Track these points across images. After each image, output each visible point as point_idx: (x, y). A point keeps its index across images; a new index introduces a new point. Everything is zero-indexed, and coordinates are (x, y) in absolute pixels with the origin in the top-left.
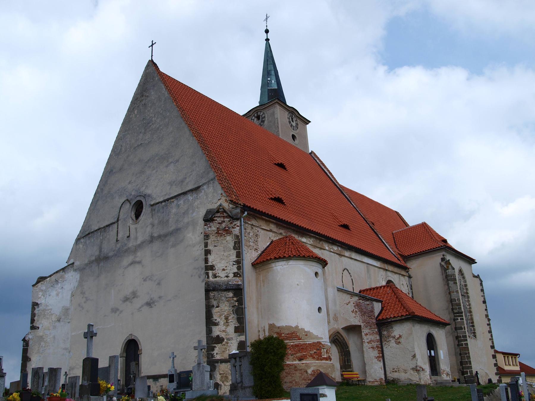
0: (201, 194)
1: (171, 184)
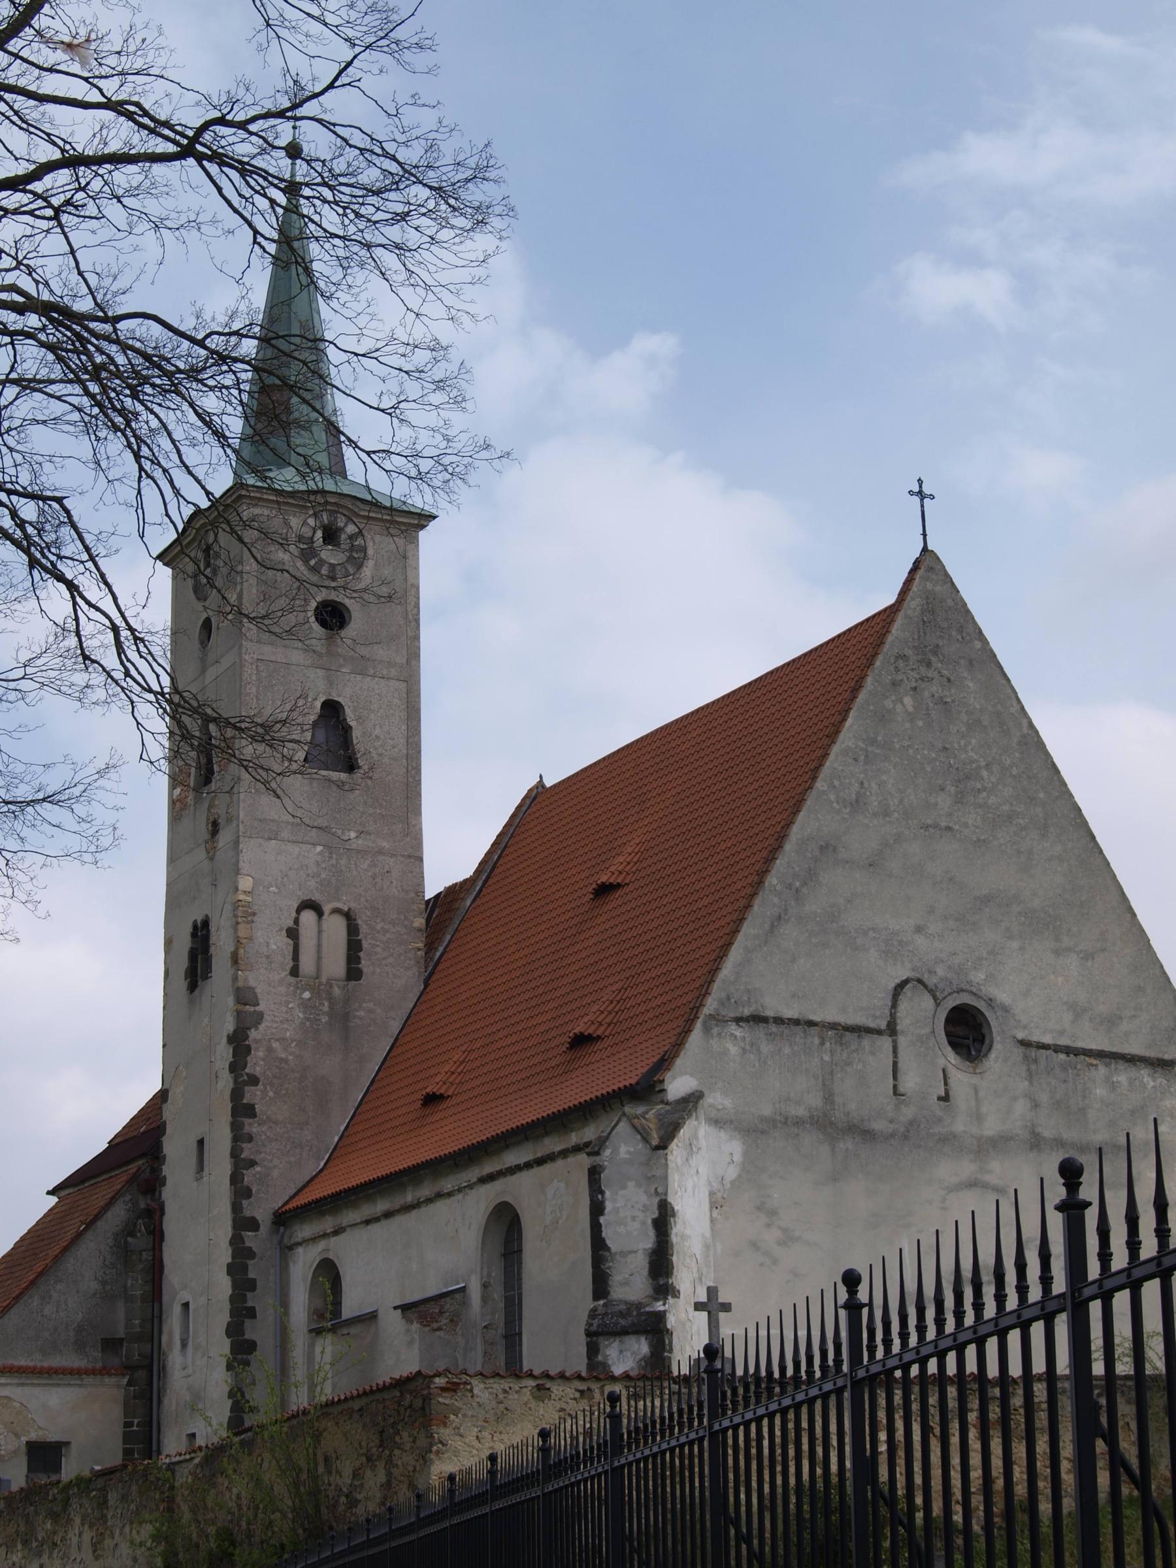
1: (1078, 1012)
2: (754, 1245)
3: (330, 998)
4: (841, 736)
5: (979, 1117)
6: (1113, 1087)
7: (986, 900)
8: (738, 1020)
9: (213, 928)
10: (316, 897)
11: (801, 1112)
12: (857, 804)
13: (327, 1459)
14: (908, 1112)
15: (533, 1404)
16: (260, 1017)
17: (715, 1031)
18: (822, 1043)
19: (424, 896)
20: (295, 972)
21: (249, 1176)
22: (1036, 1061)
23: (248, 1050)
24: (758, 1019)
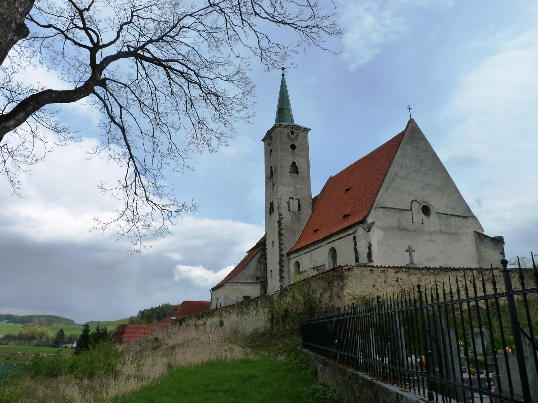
3: (296, 214)
4: (397, 153)
6: (456, 221)
7: (428, 185)
8: (381, 208)
9: (274, 203)
10: (292, 196)
11: (394, 226)
12: (401, 166)
13: (313, 291)
14: (416, 226)
15: (370, 274)
16: (283, 218)
17: (376, 210)
18: (398, 212)
19: (311, 196)
20: (289, 210)
21: (282, 247)
22: (440, 216)
23: (281, 224)
24: (385, 208)
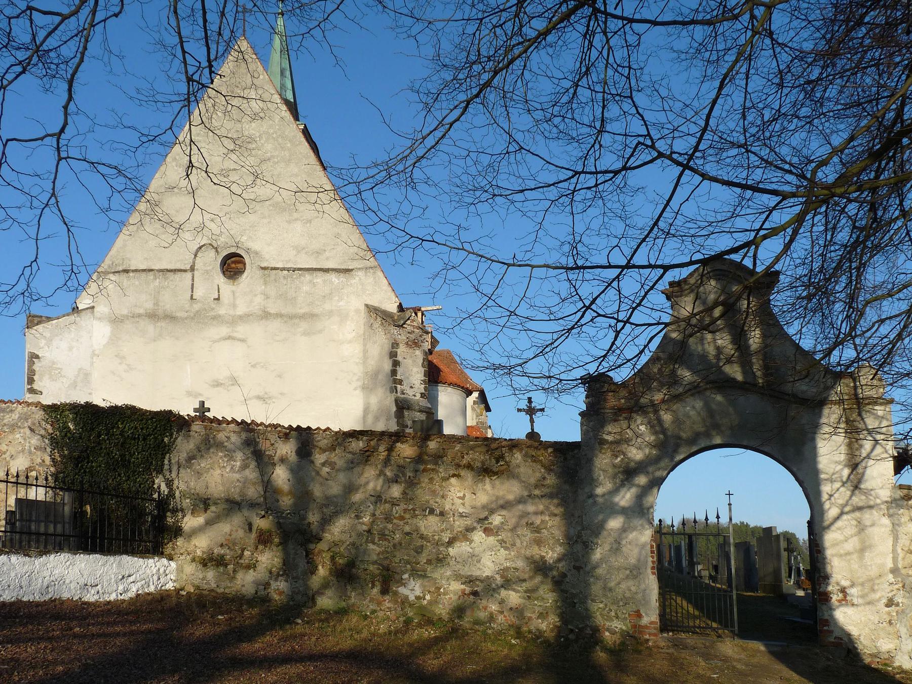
0: (353, 281)
1: (299, 249)
2: (113, 373)
5: (234, 306)
11: (142, 311)
14: (196, 307)
24: (126, 271)
